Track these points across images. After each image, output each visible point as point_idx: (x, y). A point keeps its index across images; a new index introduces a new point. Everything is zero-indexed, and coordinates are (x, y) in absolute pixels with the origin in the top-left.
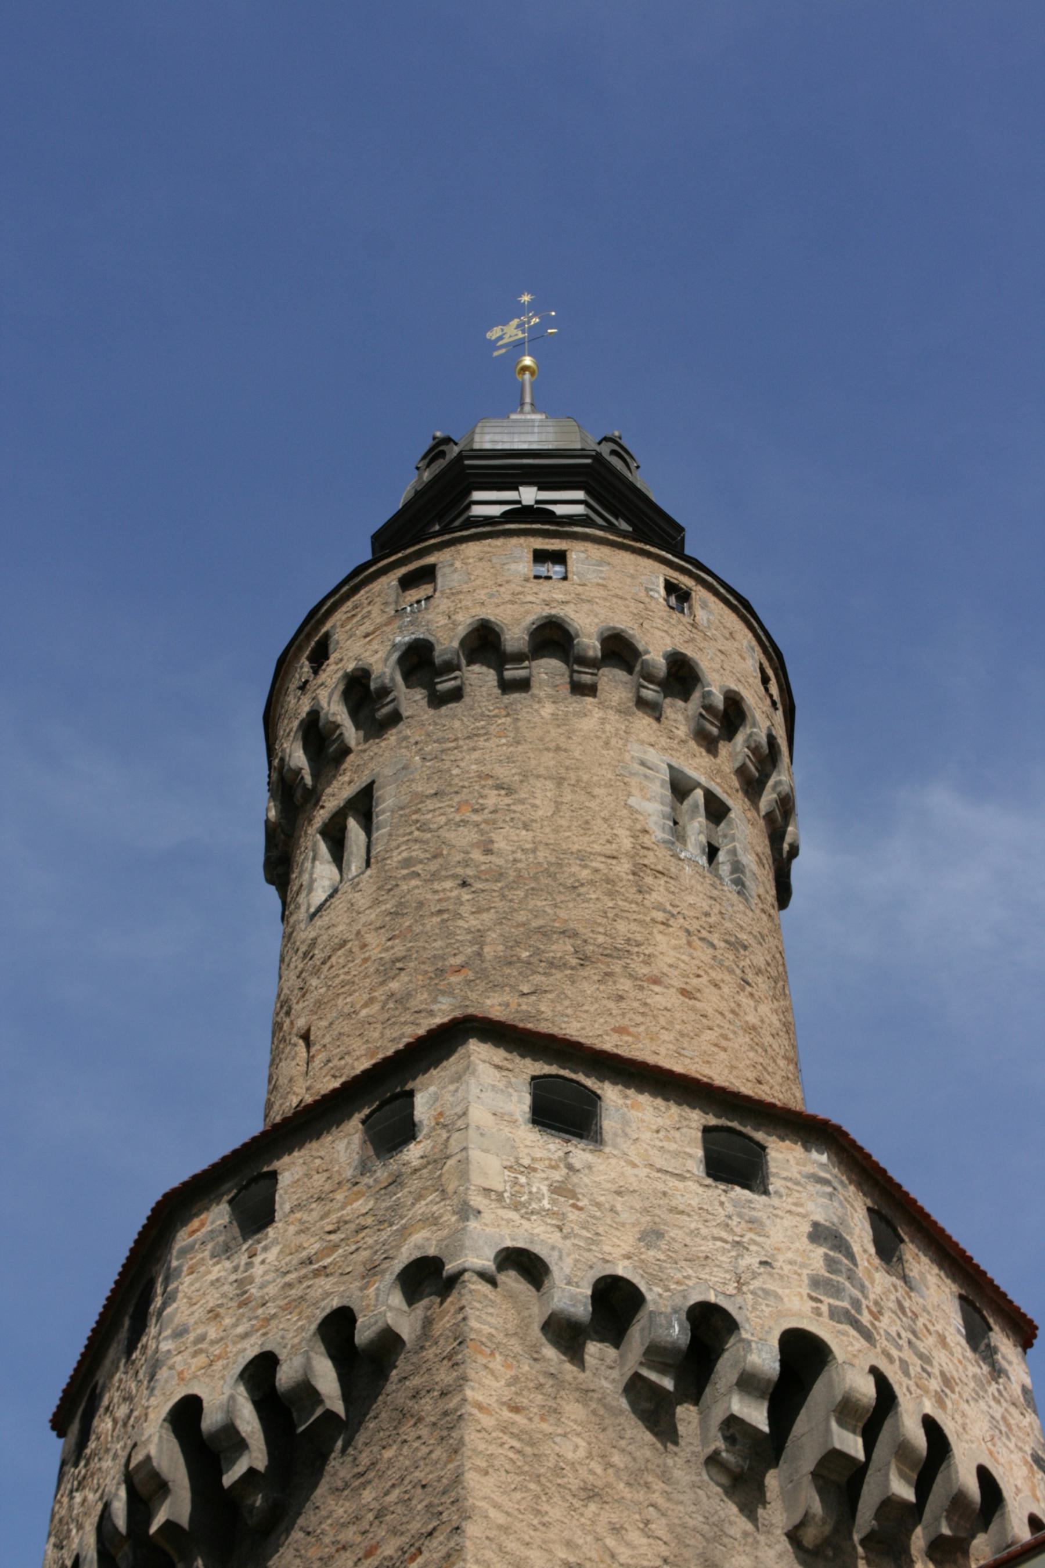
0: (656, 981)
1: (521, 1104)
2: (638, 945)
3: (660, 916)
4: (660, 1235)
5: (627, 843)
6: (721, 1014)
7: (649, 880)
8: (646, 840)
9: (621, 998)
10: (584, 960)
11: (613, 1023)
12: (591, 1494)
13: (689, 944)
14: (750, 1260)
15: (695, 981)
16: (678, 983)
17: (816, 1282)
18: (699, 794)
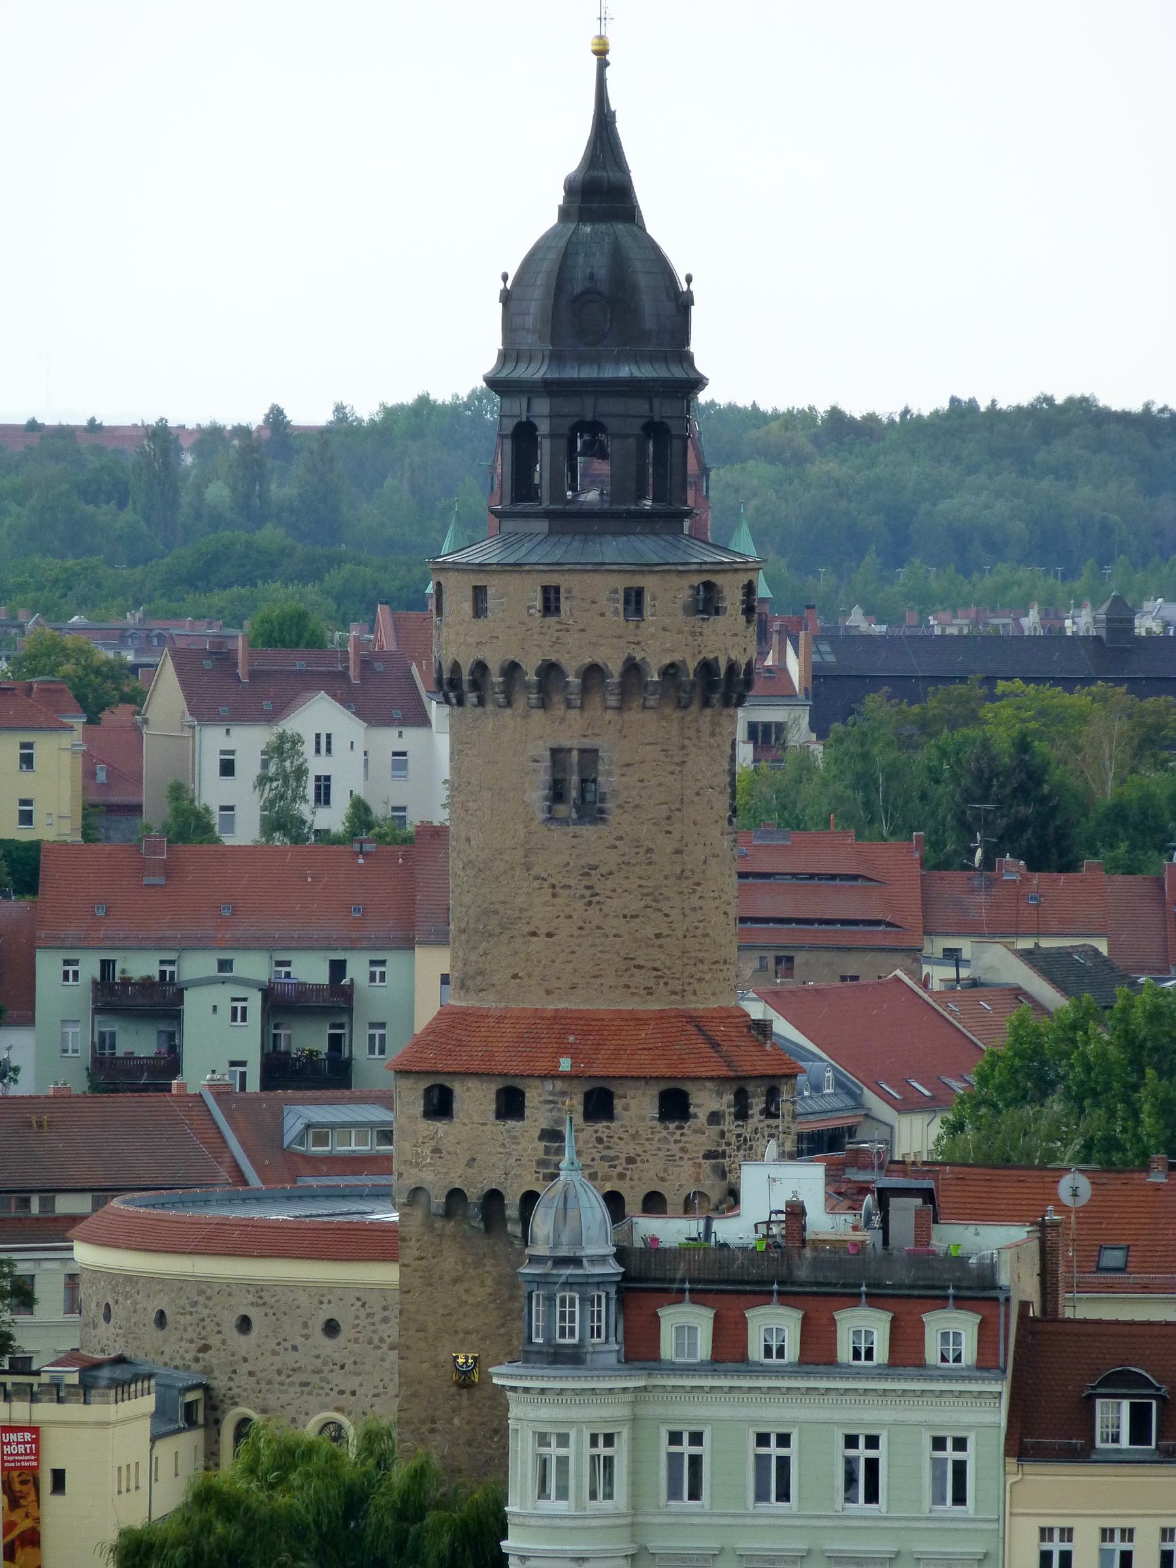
0: (534, 934)
1: (419, 1108)
2: (526, 910)
3: (537, 884)
4: (474, 1160)
5: (522, 833)
6: (572, 936)
7: (533, 858)
8: (533, 827)
9: (516, 953)
10: (503, 928)
11: (512, 971)
12: (457, 1280)
13: (554, 895)
14: (512, 1161)
15: (556, 922)
16: (543, 931)
17: (541, 1163)
18: (575, 753)
